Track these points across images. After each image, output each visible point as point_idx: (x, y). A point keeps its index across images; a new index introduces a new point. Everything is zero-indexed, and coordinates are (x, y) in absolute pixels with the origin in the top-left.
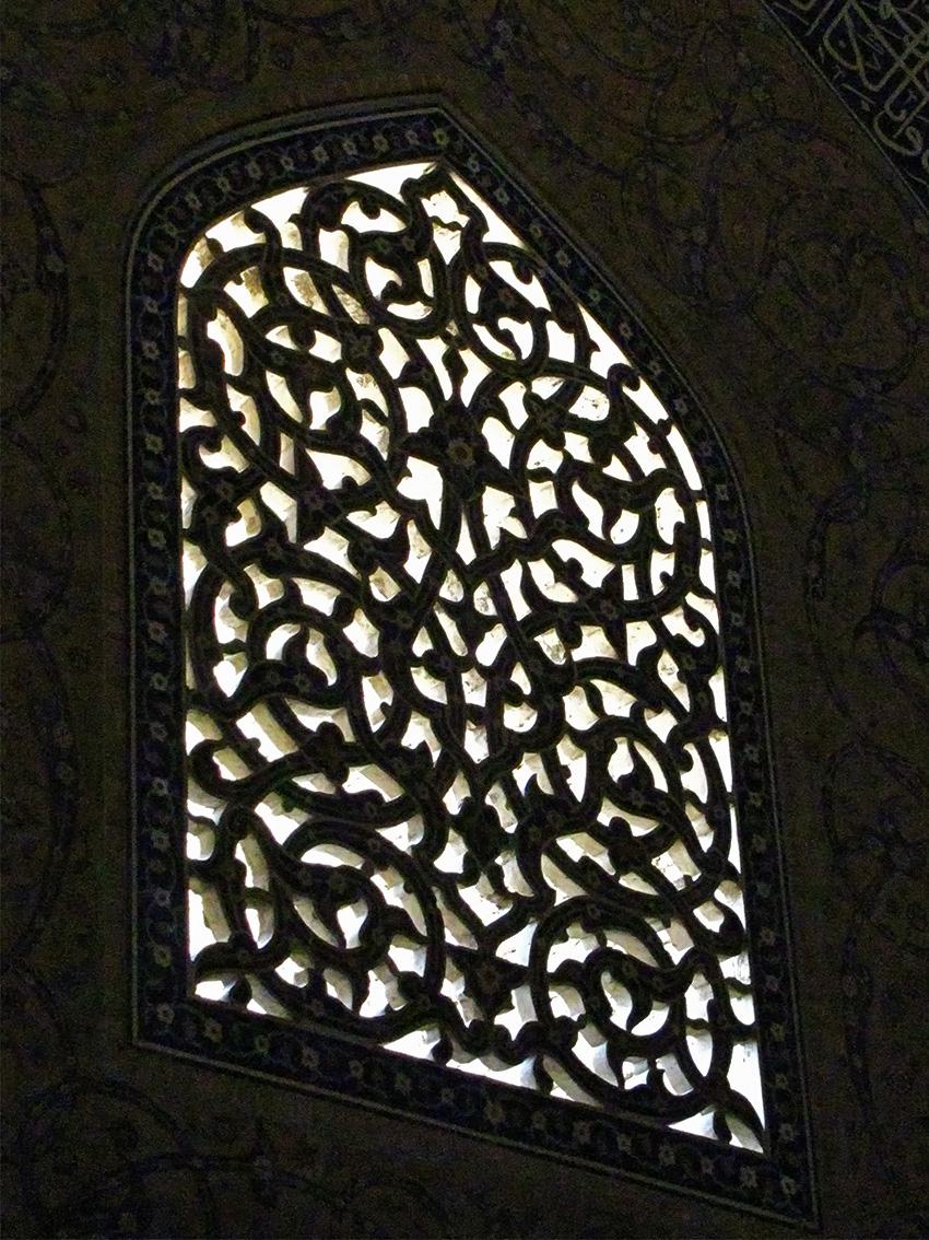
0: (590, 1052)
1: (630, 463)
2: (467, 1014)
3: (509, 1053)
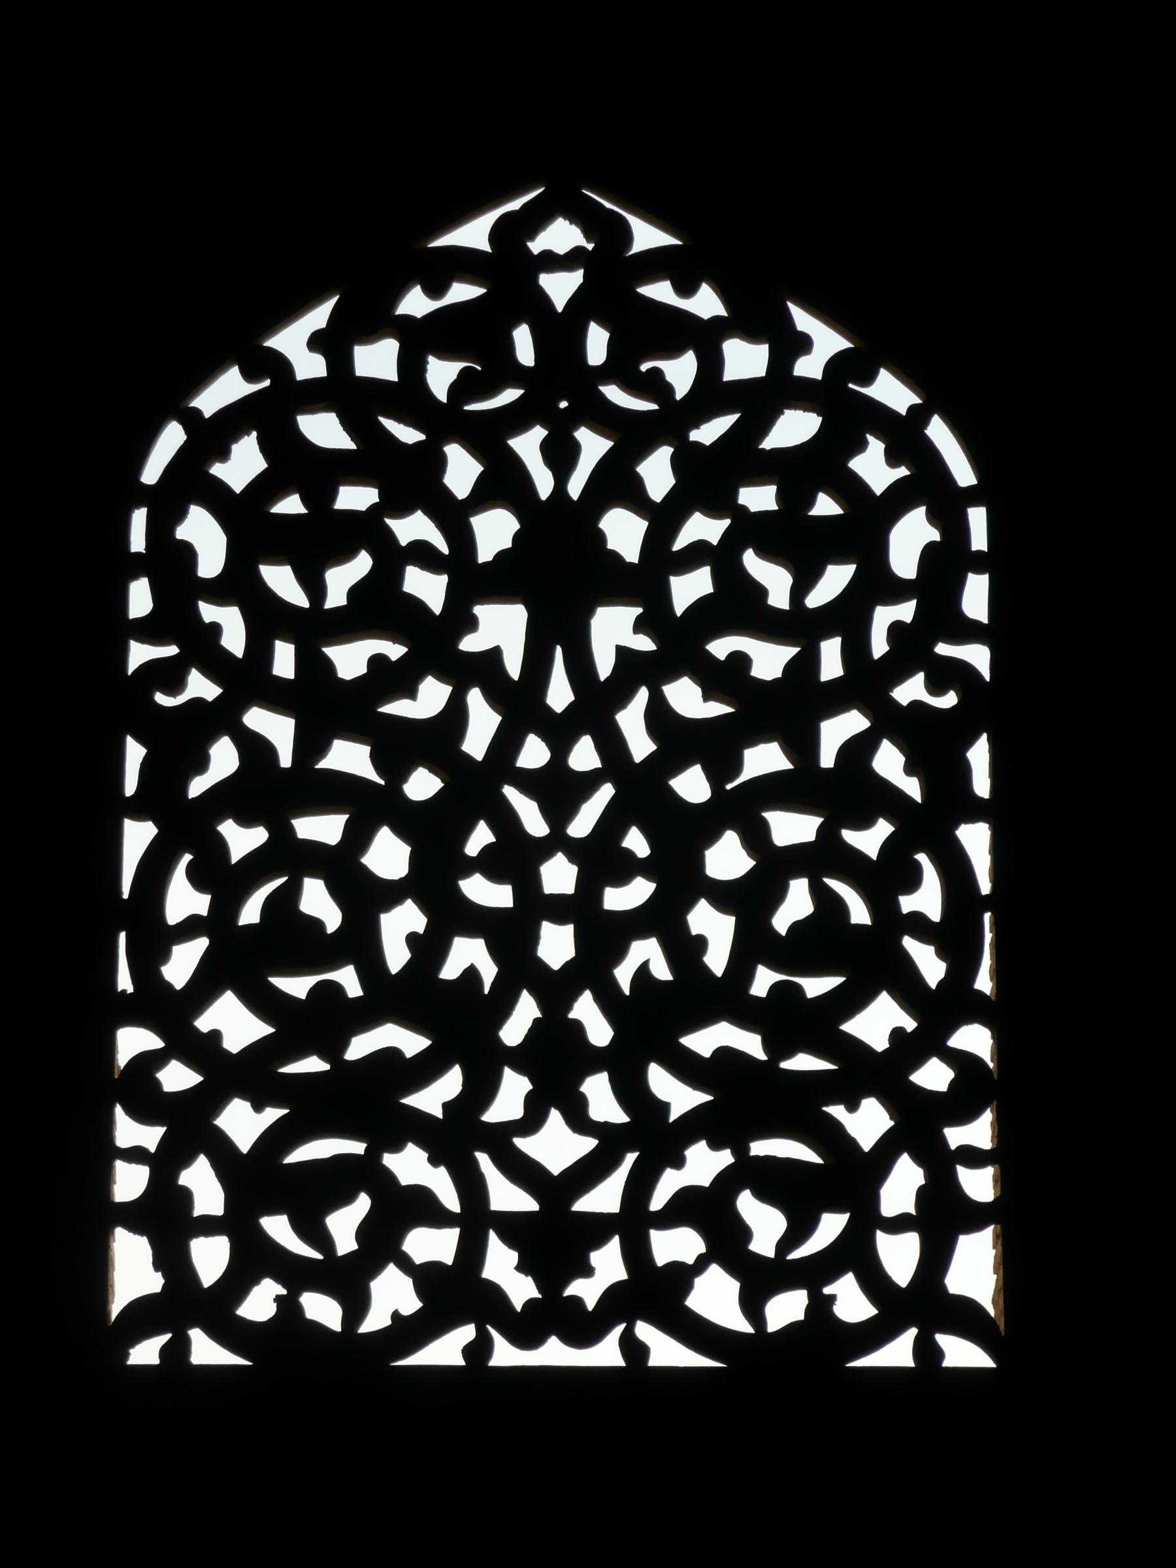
0: (716, 1297)
1: (851, 489)
2: (521, 1290)
3: (582, 1327)
